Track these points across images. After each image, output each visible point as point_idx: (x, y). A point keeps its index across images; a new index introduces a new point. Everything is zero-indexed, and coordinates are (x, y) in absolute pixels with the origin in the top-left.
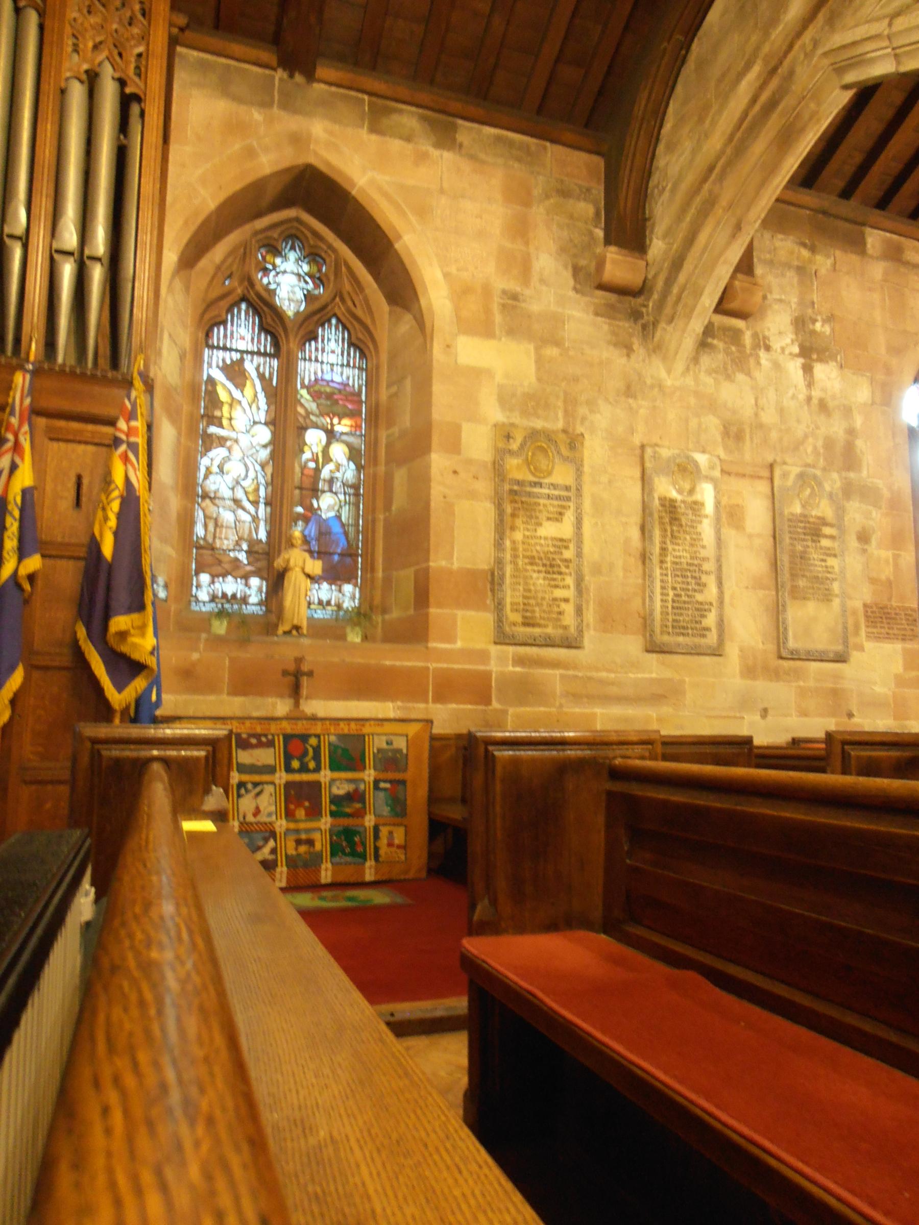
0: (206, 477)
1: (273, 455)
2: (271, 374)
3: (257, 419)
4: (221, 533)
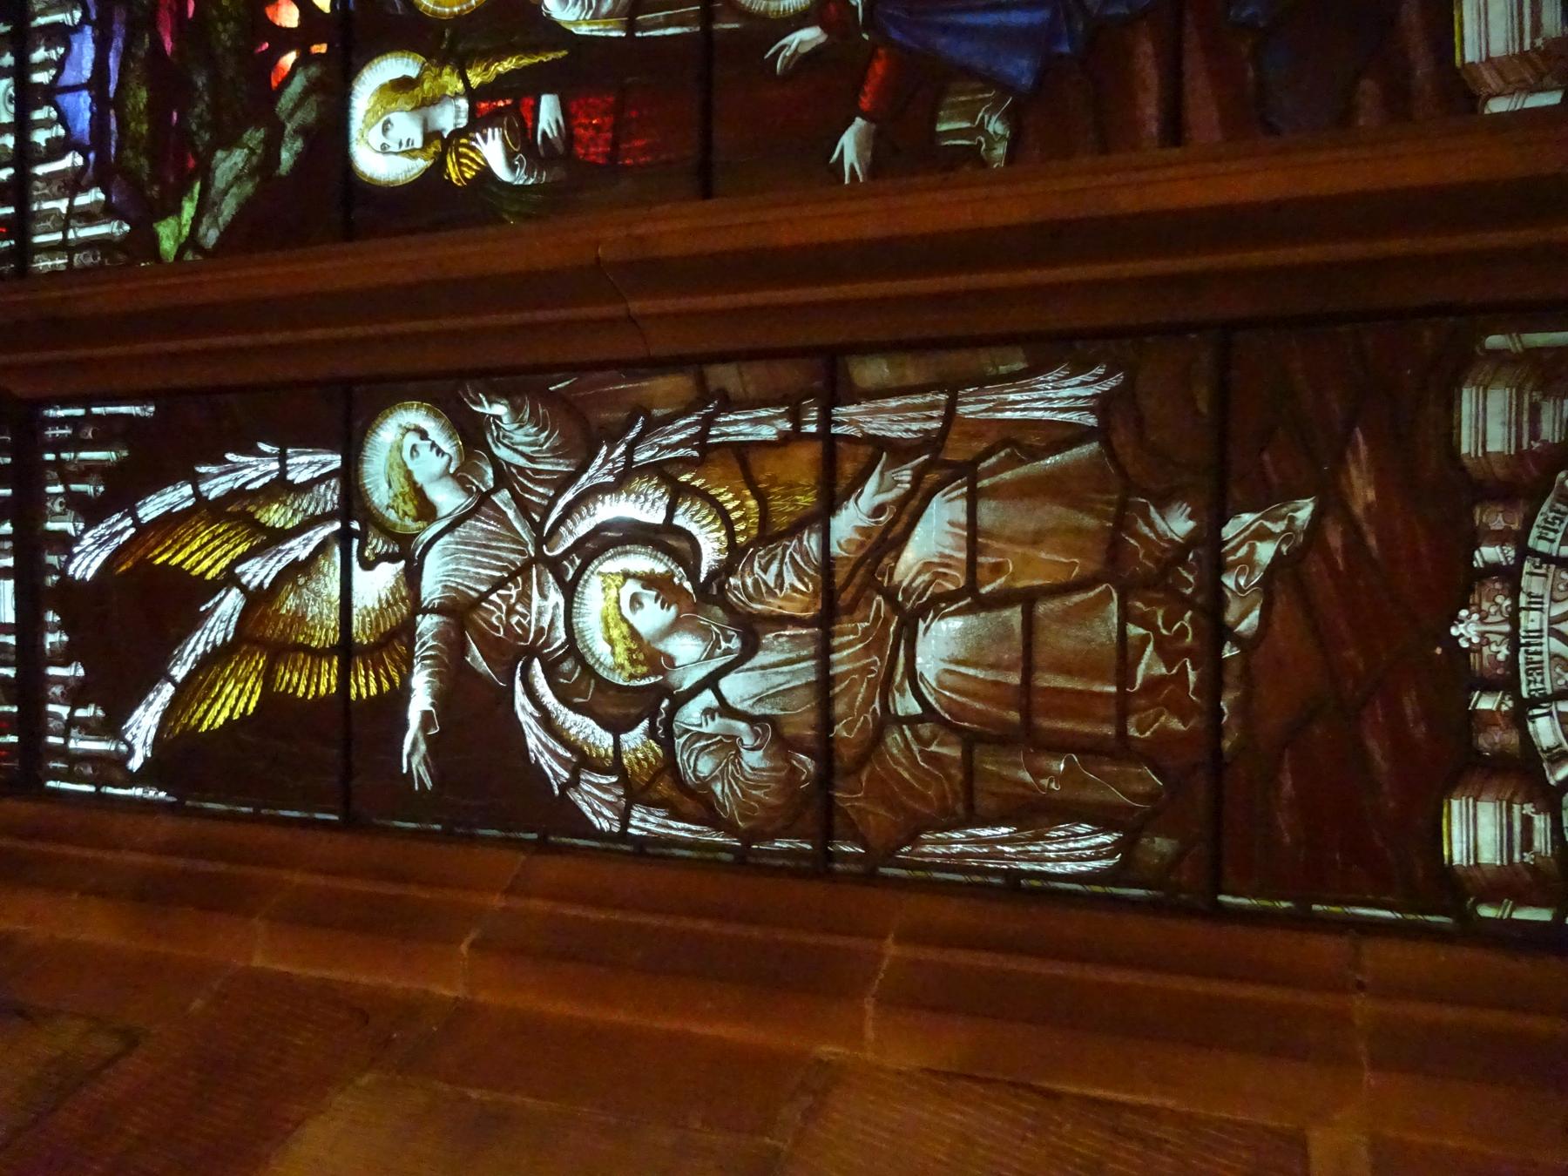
0: (694, 801)
1: (512, 383)
2: (108, 432)
3: (330, 496)
4: (1080, 704)
